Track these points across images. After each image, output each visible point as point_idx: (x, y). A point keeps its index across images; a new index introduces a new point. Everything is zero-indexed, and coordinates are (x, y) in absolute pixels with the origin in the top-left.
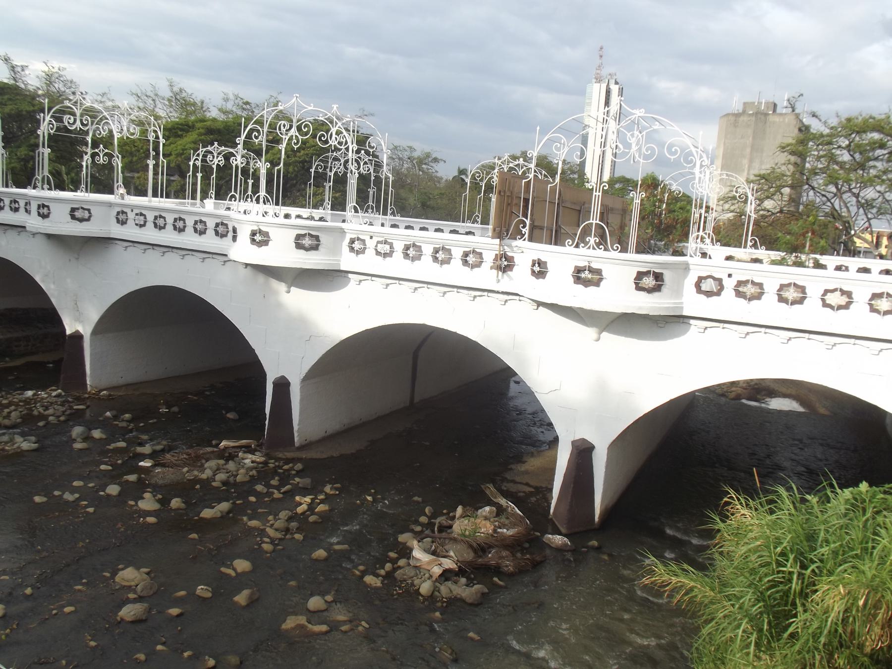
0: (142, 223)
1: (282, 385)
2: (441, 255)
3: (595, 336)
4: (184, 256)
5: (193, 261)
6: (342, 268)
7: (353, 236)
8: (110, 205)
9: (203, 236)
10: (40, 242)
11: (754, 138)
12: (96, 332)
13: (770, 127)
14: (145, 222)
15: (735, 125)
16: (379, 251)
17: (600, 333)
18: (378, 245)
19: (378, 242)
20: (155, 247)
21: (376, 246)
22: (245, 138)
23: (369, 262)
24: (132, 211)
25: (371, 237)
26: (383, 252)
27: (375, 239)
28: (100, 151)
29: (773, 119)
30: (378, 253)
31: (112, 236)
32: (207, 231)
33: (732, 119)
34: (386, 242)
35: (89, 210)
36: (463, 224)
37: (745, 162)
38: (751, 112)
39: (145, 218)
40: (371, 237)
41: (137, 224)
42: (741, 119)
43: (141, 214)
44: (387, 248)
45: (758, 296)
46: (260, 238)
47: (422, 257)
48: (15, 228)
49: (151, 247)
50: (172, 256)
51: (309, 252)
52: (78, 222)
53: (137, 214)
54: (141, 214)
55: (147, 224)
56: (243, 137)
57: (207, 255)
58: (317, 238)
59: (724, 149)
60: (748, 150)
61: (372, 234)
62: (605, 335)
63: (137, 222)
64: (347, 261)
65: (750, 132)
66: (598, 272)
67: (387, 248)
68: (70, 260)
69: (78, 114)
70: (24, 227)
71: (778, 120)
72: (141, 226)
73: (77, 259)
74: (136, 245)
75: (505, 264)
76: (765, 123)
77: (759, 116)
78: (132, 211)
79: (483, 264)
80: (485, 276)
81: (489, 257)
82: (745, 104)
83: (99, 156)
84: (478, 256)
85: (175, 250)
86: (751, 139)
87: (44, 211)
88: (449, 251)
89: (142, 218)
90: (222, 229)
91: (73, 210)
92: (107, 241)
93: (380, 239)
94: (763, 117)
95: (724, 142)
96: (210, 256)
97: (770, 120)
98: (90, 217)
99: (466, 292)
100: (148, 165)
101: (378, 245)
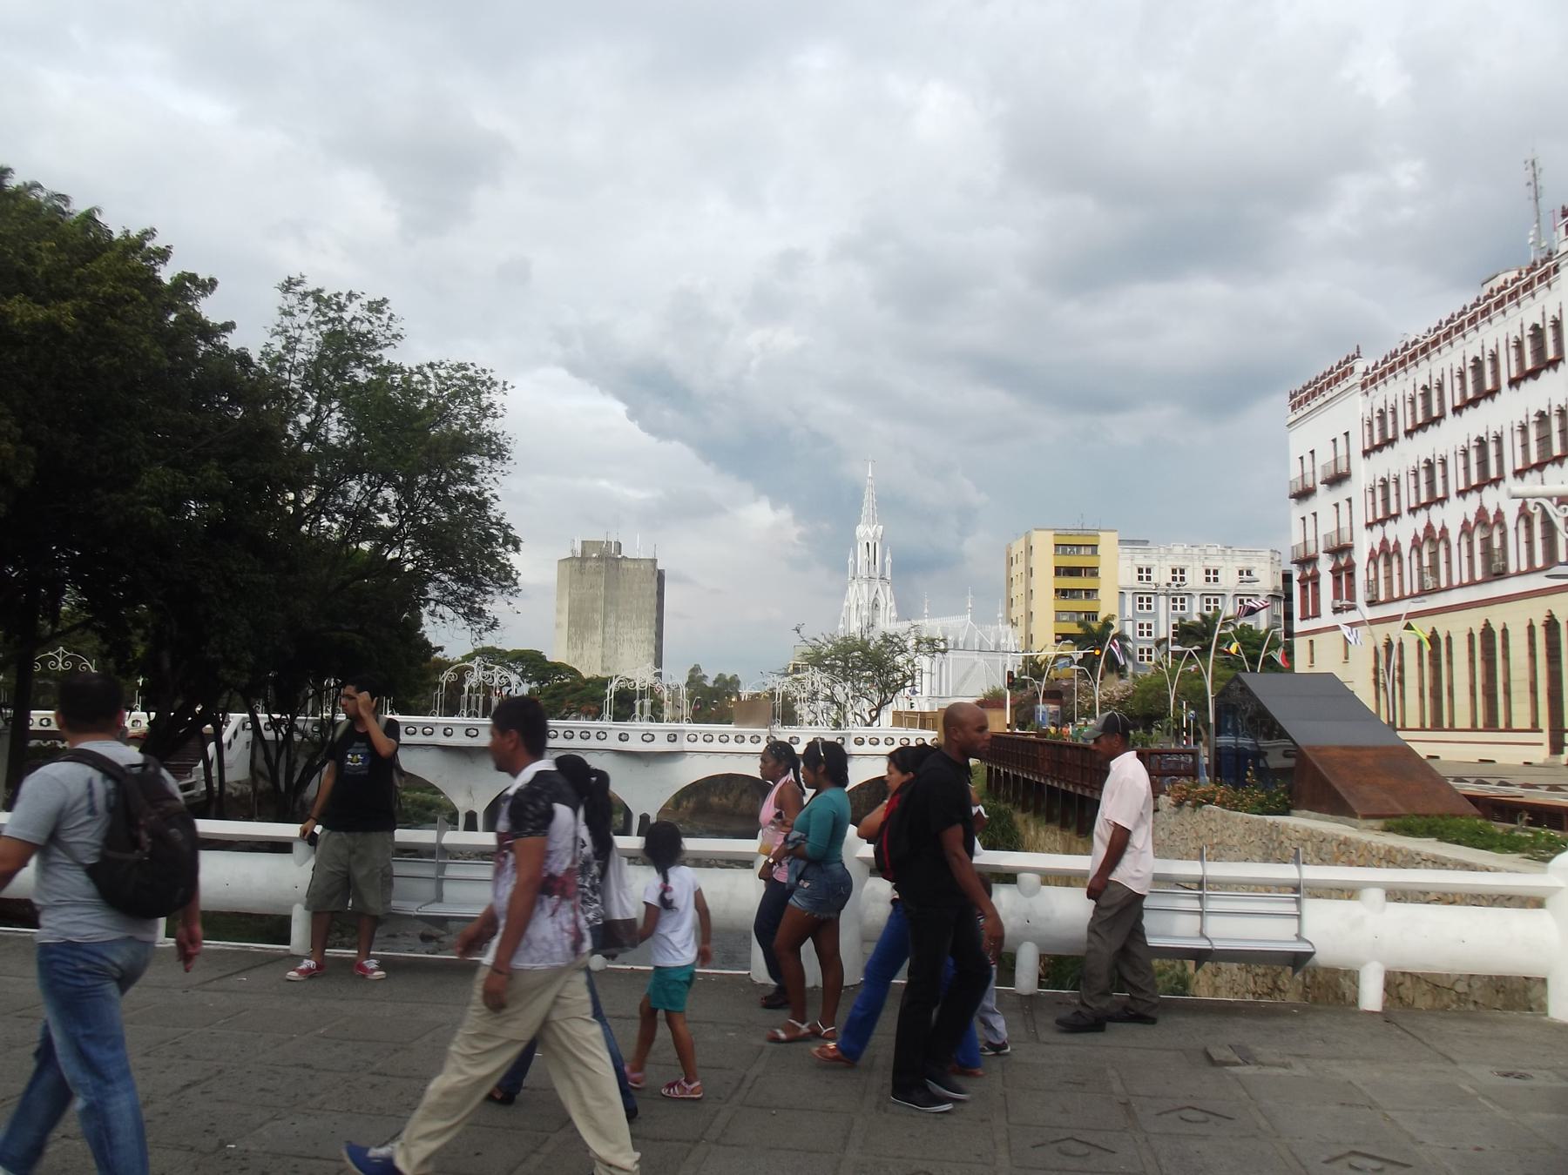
2: (740, 739)
6: (686, 750)
15: (581, 571)
23: (700, 745)
27: (703, 735)
29: (624, 564)
33: (577, 564)
37: (598, 617)
38: (594, 555)
42: (588, 564)
45: (877, 743)
46: (623, 737)
60: (601, 603)
64: (687, 746)
65: (601, 580)
71: (632, 566)
76: (618, 570)
77: (610, 561)
82: (583, 542)
86: (602, 588)
97: (623, 566)
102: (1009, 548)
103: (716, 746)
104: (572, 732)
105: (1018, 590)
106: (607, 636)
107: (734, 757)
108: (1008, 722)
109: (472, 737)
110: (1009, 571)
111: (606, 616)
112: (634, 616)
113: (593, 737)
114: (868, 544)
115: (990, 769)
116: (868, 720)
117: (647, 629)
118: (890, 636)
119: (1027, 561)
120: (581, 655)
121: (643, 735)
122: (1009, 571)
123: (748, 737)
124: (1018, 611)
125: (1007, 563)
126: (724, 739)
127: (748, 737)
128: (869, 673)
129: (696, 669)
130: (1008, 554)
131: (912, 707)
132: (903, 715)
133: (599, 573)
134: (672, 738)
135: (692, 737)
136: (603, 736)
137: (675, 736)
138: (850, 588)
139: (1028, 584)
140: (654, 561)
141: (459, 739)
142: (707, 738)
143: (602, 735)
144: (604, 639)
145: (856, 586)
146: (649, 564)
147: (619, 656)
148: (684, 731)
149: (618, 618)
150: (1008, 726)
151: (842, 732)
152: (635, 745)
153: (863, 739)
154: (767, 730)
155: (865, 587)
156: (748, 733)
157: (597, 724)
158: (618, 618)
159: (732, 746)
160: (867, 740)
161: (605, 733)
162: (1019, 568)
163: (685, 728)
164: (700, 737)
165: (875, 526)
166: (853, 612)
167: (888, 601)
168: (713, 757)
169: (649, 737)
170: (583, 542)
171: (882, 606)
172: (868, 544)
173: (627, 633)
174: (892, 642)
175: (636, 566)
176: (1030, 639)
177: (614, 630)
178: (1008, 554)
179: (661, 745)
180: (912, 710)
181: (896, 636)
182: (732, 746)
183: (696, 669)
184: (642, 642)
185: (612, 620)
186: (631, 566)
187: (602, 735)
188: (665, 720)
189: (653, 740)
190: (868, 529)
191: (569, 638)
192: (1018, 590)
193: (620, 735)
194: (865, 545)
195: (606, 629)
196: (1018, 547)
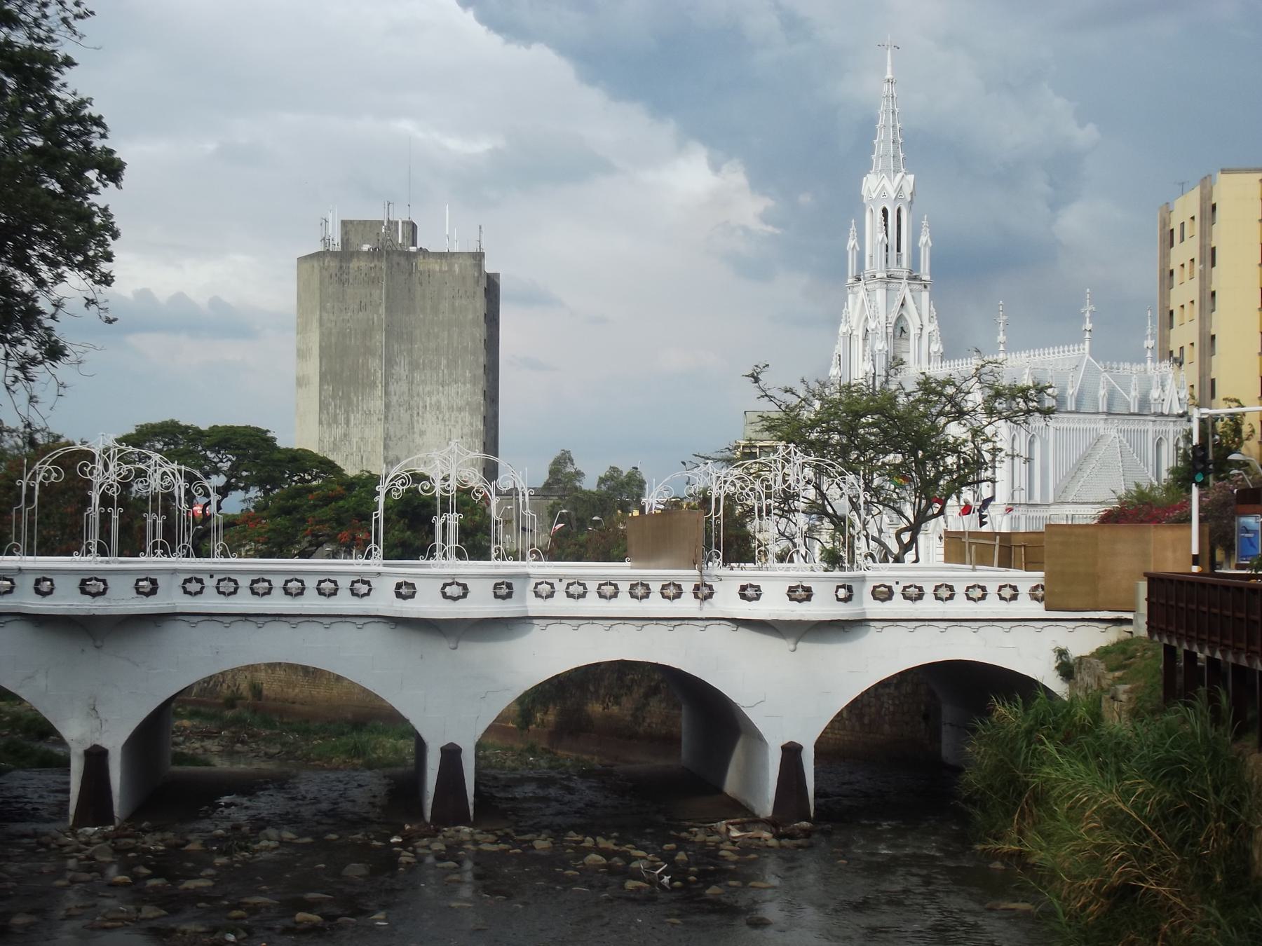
1: (451, 754)
2: (640, 591)
3: (792, 647)
6: (531, 614)
11: (389, 310)
13: (421, 284)
15: (342, 278)
17: (796, 644)
21: (568, 588)
23: (560, 604)
25: (560, 580)
27: (565, 582)
29: (422, 264)
30: (569, 595)
33: (333, 264)
34: (611, 584)
36: (523, 563)
37: (376, 365)
38: (366, 247)
40: (560, 580)
42: (354, 264)
46: (405, 591)
47: (619, 595)
52: (144, 597)
59: (322, 334)
60: (380, 338)
62: (800, 644)
64: (534, 606)
65: (379, 294)
66: (808, 590)
68: (83, 650)
71: (437, 268)
75: (704, 592)
76: (410, 274)
77: (396, 259)
79: (683, 595)
80: (687, 605)
81: (688, 588)
82: (344, 223)
85: (284, 619)
86: (382, 310)
91: (83, 582)
94: (403, 261)
95: (321, 317)
97: (421, 268)
98: (105, 590)
99: (665, 623)
102: (1167, 210)
103: (592, 605)
105: (1185, 292)
106: (394, 399)
107: (629, 628)
108: (1195, 551)
110: (1165, 257)
111: (390, 362)
112: (444, 362)
113: (344, 592)
114: (885, 212)
115: (1170, 651)
116: (895, 548)
117: (468, 386)
118: (937, 382)
119: (1205, 234)
120: (345, 435)
121: (445, 585)
122: (1165, 257)
123: (655, 587)
124: (1185, 334)
125: (1162, 241)
126: (608, 591)
127: (655, 587)
128: (895, 458)
129: (563, 460)
130: (1165, 222)
131: (982, 524)
132: (966, 539)
133: (374, 281)
134: (504, 590)
135: (545, 588)
136: (364, 589)
137: (509, 586)
138: (850, 297)
139: (1205, 279)
140: (478, 257)
141: (67, 601)
142: (572, 589)
143: (362, 586)
144: (387, 406)
145: (862, 294)
146: (470, 262)
147: (416, 436)
148: (527, 576)
149: (414, 366)
150: (1196, 559)
151: (846, 574)
152: (429, 605)
153: (890, 588)
154: (696, 572)
155: (880, 294)
156: (656, 578)
157: (356, 564)
158: (414, 366)
159: (625, 605)
160: (897, 590)
162: (1184, 252)
163: (530, 571)
164: (560, 587)
165: (899, 176)
166: (858, 345)
167: (926, 322)
168: (587, 628)
169: (457, 590)
170: (344, 223)
171: (913, 331)
172: (885, 212)
173: (430, 394)
174: (940, 394)
175: (445, 268)
176: (1208, 389)
177: (405, 387)
178: (1165, 222)
179: (481, 605)
180: (985, 529)
181: (949, 382)
183: (563, 460)
184: (460, 409)
185: (401, 370)
186: (435, 266)
188: (494, 555)
189: (464, 596)
190: (886, 182)
191: (323, 406)
192: (1185, 292)
193: (399, 586)
194: (880, 214)
195: (392, 388)
196: (1187, 207)
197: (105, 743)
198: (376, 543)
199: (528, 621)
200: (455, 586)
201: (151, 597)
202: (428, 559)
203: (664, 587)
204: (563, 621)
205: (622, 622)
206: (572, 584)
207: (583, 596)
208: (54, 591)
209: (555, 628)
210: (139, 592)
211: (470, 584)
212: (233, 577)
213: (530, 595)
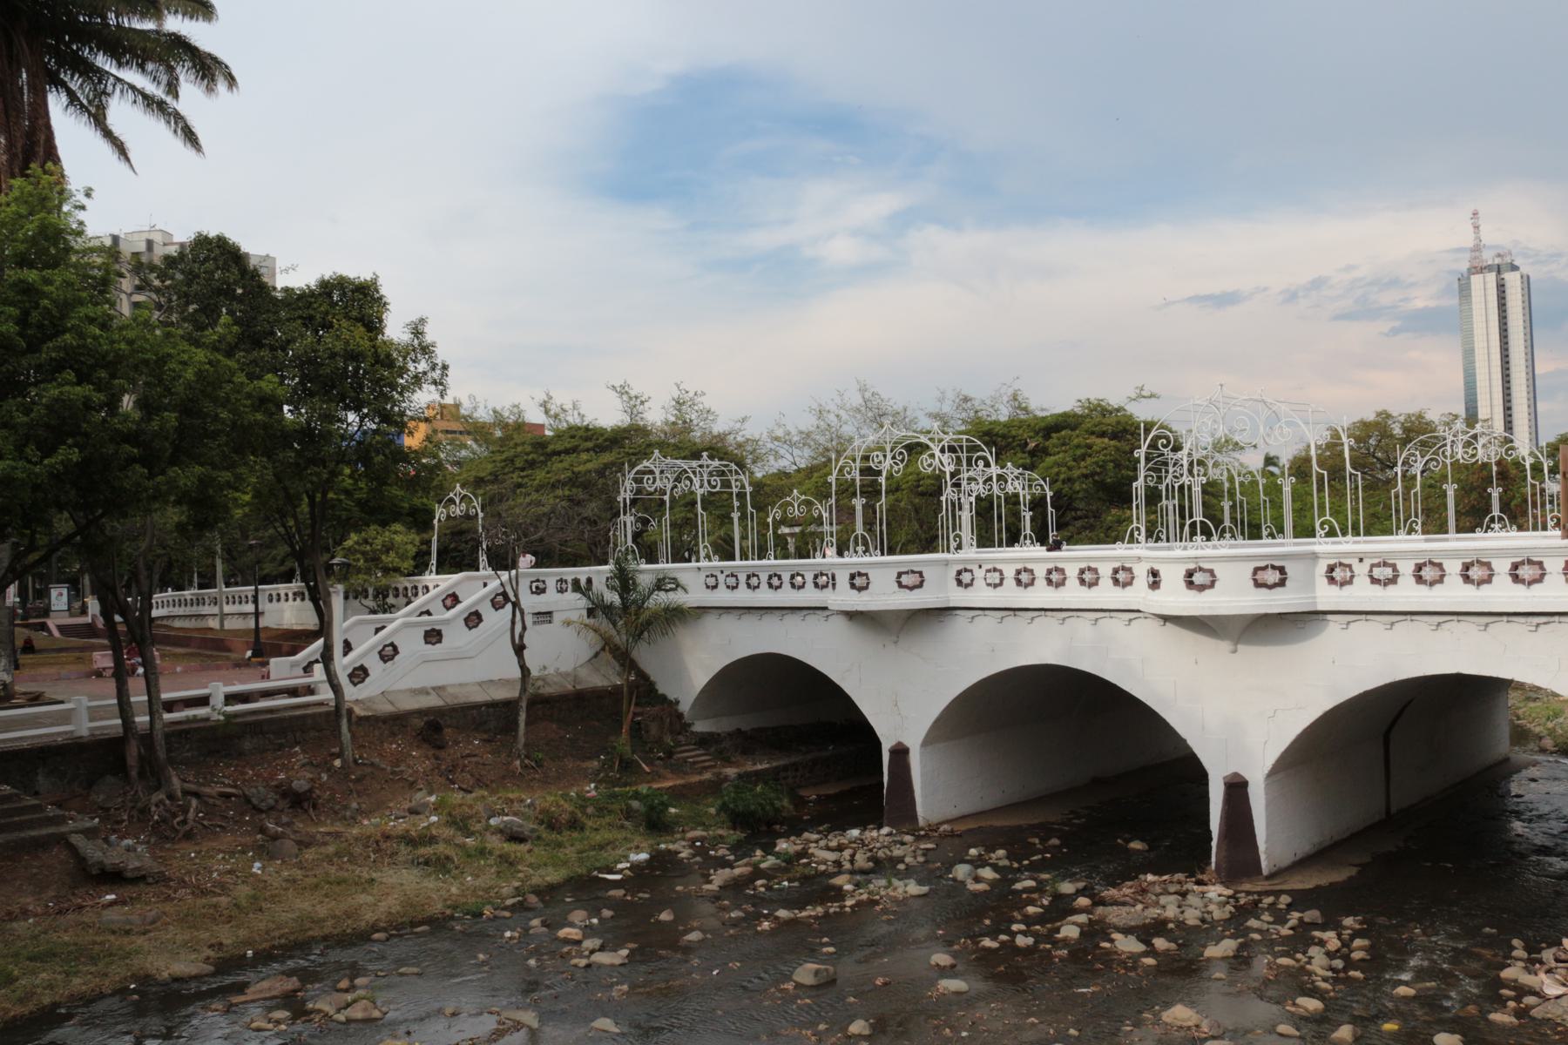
0: (997, 581)
1: (1237, 789)
4: (1064, 619)
5: (1082, 625)
6: (1320, 608)
7: (1332, 562)
8: (947, 563)
9: (1095, 588)
10: (840, 623)
12: (928, 742)
14: (1002, 580)
16: (1376, 577)
18: (1374, 569)
19: (1373, 566)
20: (1017, 613)
21: (1371, 571)
22: (1148, 448)
23: (1362, 594)
24: (980, 567)
25: (1361, 560)
26: (1382, 578)
27: (1367, 563)
28: (798, 498)
30: (1374, 581)
31: (951, 605)
32: (1100, 582)
35: (920, 574)
39: (1001, 574)
40: (1361, 560)
41: (989, 585)
43: (995, 570)
44: (1388, 572)
48: (798, 612)
49: (1011, 613)
50: (1043, 621)
51: (1273, 591)
52: (908, 591)
53: (988, 571)
54: (995, 570)
55: (1005, 582)
56: (1144, 448)
57: (1102, 614)
58: (1282, 570)
61: (1361, 556)
63: (988, 581)
64: (1326, 596)
67: (1388, 572)
69: (888, 449)
70: (825, 608)
72: (996, 586)
73: (896, 642)
74: (987, 612)
78: (980, 567)
79: (1546, 577)
83: (793, 507)
84: (1537, 567)
85: (1049, 613)
87: (859, 581)
88: (1488, 565)
89: (997, 574)
90: (1124, 576)
92: (942, 613)
93: (1376, 561)
96: (1107, 614)
99: (1522, 619)
100: (853, 508)
101: (1374, 569)
104: (1211, 572)
107: (1468, 627)
109: (911, 588)
113: (1105, 581)
126: (1475, 572)
134: (1272, 576)
142: (1377, 572)
148: (1314, 557)
157: (1119, 551)
161: (1440, 566)
163: (1317, 548)
164: (1361, 570)
182: (1407, 594)
187: (824, 581)
188: (1265, 533)
197: (908, 743)
198: (1416, 516)
199: (1321, 617)
200: (911, 575)
201: (916, 591)
202: (1486, 532)
203: (1515, 566)
204: (1369, 617)
205: (1455, 618)
206: (1378, 565)
207: (1393, 580)
208: (925, 584)
209: (1360, 627)
210: (900, 585)
211: (1219, 569)
212: (999, 566)
213: (1322, 581)
